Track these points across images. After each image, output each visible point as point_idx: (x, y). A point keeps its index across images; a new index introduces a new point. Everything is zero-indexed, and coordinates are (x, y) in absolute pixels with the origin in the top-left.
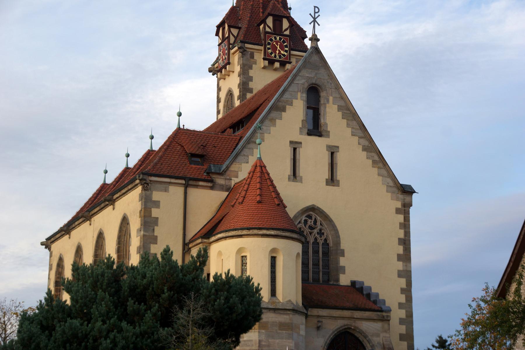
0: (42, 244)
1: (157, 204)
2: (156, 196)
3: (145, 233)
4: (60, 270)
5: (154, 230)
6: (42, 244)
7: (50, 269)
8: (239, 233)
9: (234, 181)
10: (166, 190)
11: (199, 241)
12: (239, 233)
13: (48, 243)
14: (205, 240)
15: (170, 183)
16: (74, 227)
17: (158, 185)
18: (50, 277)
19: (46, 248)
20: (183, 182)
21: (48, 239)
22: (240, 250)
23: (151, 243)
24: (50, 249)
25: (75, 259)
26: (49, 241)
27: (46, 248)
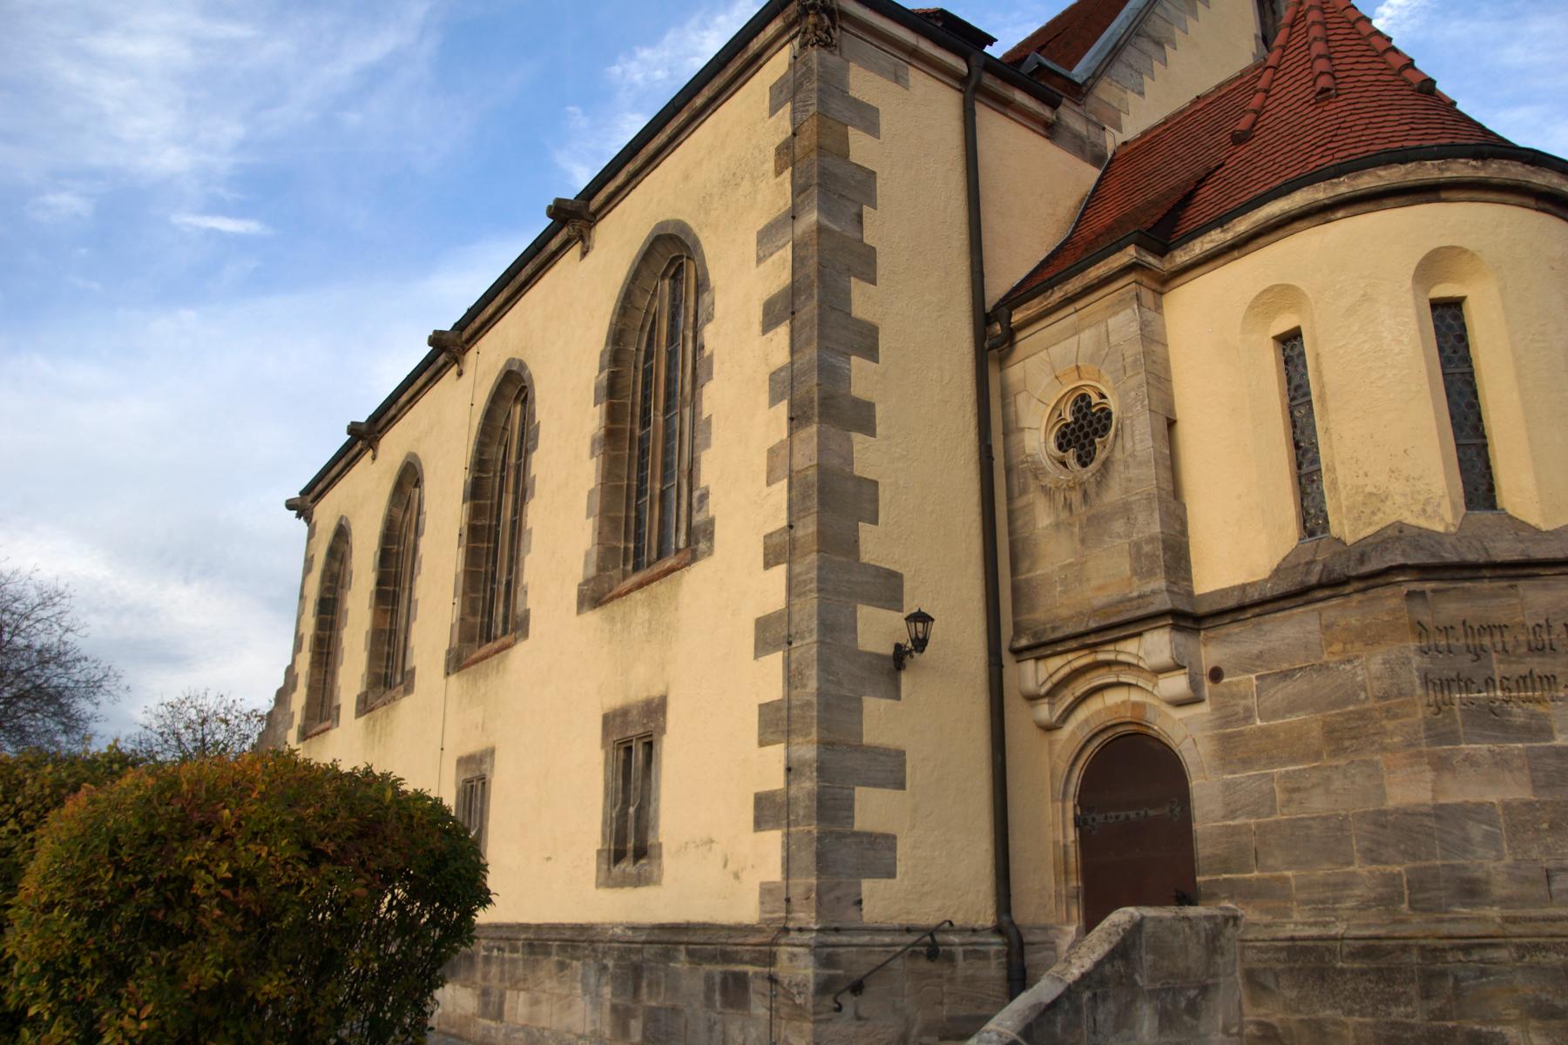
0: (290, 505)
1: (868, 118)
2: (864, 83)
3: (826, 222)
4: (336, 565)
5: (859, 218)
6: (290, 505)
7: (308, 569)
8: (1429, 171)
9: (1112, 141)
10: (898, 79)
11: (1130, 254)
12: (1429, 171)
13: (303, 506)
14: (1150, 259)
15: (914, 54)
16: (394, 417)
17: (868, 48)
18: (306, 592)
19: (299, 516)
20: (960, 65)
21: (306, 492)
22: (1433, 264)
23: (849, 271)
24: (308, 520)
25: (390, 510)
26: (309, 498)
27: (299, 516)
